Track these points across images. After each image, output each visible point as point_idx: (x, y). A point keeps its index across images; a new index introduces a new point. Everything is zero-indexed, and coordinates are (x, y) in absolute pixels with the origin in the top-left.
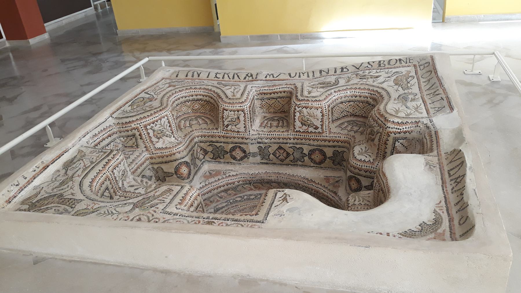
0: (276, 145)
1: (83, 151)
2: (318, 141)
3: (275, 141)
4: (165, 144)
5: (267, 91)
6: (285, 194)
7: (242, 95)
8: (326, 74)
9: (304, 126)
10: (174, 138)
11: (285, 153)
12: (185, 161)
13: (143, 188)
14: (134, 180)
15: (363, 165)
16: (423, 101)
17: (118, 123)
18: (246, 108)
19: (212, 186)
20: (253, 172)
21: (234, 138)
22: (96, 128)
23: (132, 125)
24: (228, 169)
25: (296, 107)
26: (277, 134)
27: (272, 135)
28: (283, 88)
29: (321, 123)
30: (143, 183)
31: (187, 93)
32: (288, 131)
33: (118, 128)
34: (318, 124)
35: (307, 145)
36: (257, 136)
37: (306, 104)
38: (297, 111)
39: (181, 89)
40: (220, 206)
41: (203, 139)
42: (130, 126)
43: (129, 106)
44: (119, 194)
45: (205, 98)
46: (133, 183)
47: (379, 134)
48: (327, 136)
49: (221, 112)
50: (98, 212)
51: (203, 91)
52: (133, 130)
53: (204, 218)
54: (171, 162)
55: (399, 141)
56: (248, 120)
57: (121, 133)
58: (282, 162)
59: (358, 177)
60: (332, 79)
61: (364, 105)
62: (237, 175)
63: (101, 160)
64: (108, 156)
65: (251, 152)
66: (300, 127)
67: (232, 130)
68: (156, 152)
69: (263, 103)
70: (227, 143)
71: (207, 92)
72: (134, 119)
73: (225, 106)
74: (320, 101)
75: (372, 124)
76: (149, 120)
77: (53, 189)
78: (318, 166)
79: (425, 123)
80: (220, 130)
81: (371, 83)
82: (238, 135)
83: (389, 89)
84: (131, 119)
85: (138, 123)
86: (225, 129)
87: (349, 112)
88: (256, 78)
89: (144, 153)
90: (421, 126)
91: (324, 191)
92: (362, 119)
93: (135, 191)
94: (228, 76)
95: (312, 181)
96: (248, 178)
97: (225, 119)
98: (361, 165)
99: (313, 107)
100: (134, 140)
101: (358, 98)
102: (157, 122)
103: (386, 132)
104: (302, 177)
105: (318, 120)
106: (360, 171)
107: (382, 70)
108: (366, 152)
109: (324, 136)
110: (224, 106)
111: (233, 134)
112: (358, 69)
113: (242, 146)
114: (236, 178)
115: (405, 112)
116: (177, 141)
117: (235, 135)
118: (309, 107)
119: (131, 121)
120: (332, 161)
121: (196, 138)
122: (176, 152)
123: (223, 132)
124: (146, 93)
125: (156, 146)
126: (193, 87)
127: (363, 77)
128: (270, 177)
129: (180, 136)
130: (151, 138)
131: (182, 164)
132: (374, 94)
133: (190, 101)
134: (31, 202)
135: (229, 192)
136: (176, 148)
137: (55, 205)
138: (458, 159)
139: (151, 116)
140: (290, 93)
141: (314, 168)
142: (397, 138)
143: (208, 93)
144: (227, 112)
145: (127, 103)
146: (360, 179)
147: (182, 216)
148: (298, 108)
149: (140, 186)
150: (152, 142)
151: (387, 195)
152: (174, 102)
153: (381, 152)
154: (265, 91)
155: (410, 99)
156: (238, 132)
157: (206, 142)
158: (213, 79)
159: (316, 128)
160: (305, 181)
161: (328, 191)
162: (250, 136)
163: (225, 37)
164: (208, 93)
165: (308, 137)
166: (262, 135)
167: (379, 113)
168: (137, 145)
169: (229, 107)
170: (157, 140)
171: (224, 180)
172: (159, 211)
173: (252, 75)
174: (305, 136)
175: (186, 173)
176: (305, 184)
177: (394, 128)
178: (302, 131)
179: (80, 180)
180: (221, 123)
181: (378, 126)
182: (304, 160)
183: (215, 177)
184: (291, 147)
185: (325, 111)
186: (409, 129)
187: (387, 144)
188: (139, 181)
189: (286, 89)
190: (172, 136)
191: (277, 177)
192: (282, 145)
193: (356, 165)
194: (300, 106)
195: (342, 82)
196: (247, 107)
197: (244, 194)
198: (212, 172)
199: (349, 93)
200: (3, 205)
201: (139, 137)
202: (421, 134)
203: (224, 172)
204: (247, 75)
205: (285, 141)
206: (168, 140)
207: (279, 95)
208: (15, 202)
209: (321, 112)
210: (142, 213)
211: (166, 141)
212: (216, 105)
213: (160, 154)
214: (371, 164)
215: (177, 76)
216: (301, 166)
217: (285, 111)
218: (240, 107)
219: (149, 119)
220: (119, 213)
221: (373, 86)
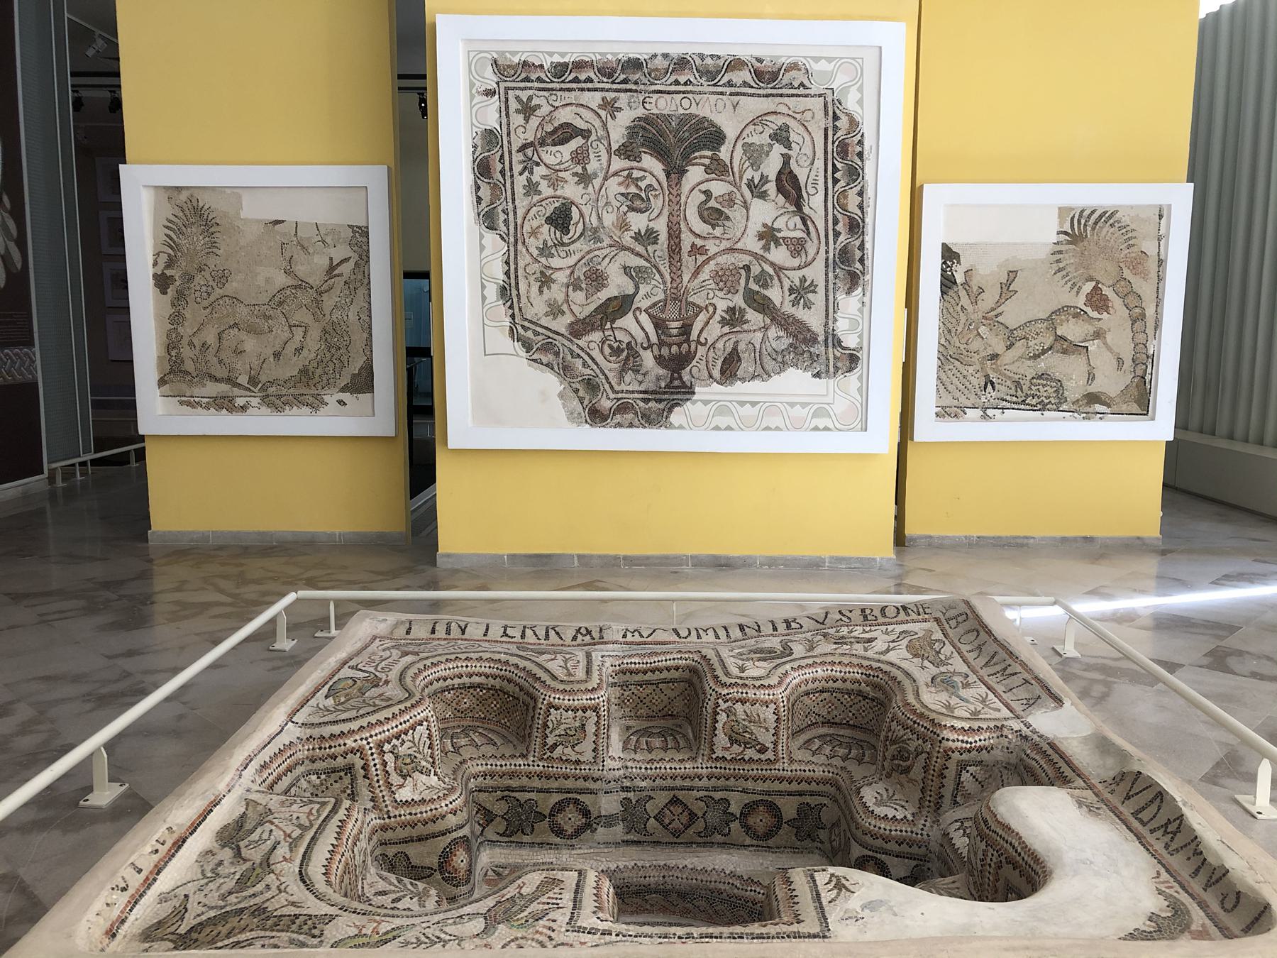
1: (259, 801)
2: (764, 782)
3: (664, 783)
5: (637, 666)
7: (587, 672)
8: (755, 633)
9: (735, 745)
11: (686, 813)
13: (411, 898)
15: (893, 828)
16: (989, 689)
17: (311, 737)
18: (602, 704)
21: (566, 777)
22: (265, 746)
23: (346, 742)
24: (541, 861)
26: (668, 767)
27: (658, 770)
28: (674, 659)
29: (773, 739)
30: (405, 885)
31: (449, 669)
32: (694, 759)
33: (308, 750)
34: (766, 739)
35: (738, 791)
37: (742, 693)
38: (721, 710)
39: (435, 660)
41: (489, 782)
42: (342, 742)
43: (326, 697)
45: (491, 681)
46: (382, 885)
48: (786, 769)
49: (542, 712)
50: (401, 939)
51: (488, 665)
53: (679, 937)
54: (433, 837)
55: (968, 768)
56: (602, 732)
57: (314, 762)
59: (883, 857)
60: (774, 643)
61: (852, 700)
63: (324, 821)
64: (336, 813)
65: (603, 813)
66: (727, 749)
67: (564, 758)
68: (397, 813)
69: (626, 693)
70: (548, 791)
71: (497, 668)
72: (354, 725)
73: (554, 698)
74: (770, 686)
75: (899, 736)
76: (388, 730)
77: (223, 897)
78: (761, 843)
79: (1015, 729)
80: (532, 759)
81: (862, 653)
82: (576, 769)
83: (904, 665)
84: (345, 727)
85: (364, 736)
86: (545, 757)
87: (819, 715)
88: (601, 637)
90: (1010, 736)
92: (848, 731)
93: (395, 905)
94: (535, 633)
95: (752, 880)
97: (550, 729)
98: (888, 828)
99: (757, 701)
100: (347, 780)
101: (839, 684)
102: (406, 735)
104: (727, 872)
105: (768, 731)
106: (886, 842)
107: (873, 628)
108: (890, 798)
109: (779, 770)
110: (552, 699)
111: (564, 770)
112: (823, 624)
113: (581, 797)
115: (965, 708)
116: (443, 785)
117: (568, 770)
118: (748, 700)
119: (346, 732)
120: (795, 830)
121: (472, 780)
122: (446, 812)
123: (541, 764)
124: (351, 668)
125: (397, 796)
126: (463, 656)
127: (840, 641)
128: (645, 877)
130: (389, 775)
131: (457, 843)
132: (874, 676)
133: (453, 689)
134: (173, 933)
136: (448, 803)
137: (254, 934)
138: (1144, 790)
139: (395, 720)
141: (751, 849)
142: (966, 761)
143: (501, 670)
144: (559, 712)
145: (317, 690)
147: (624, 936)
148: (725, 702)
149: (402, 894)
150: (389, 785)
151: (1037, 868)
152: (423, 690)
153: (930, 796)
154: (633, 665)
155: (961, 684)
156: (578, 762)
157: (495, 789)
158: (500, 639)
159: (763, 750)
160: (735, 883)
162: (605, 772)
163: (449, 556)
164: (501, 670)
165: (741, 771)
166: (634, 770)
167: (914, 712)
168: (353, 793)
169: (564, 700)
172: (561, 927)
173: (589, 632)
174: (737, 771)
177: (958, 740)
178: (728, 758)
179: (297, 870)
180: (538, 739)
181: (918, 739)
182: (730, 831)
184: (700, 799)
185: (782, 710)
186: (987, 743)
187: (945, 777)
188: (396, 882)
189: (680, 661)
190: (432, 773)
191: (664, 877)
192: (680, 795)
193: (877, 829)
194: (728, 697)
195: (798, 650)
196: (604, 701)
199: (820, 672)
200: (101, 943)
201: (362, 772)
202: (1012, 752)
204: (578, 631)
205: (687, 783)
207: (665, 674)
208: (125, 937)
209: (774, 713)
210: (520, 935)
212: (522, 697)
213: (408, 817)
214: (909, 824)
215: (408, 632)
216: (723, 845)
217: (675, 713)
218: (589, 701)
219: (390, 727)
220: (460, 940)
221: (869, 659)
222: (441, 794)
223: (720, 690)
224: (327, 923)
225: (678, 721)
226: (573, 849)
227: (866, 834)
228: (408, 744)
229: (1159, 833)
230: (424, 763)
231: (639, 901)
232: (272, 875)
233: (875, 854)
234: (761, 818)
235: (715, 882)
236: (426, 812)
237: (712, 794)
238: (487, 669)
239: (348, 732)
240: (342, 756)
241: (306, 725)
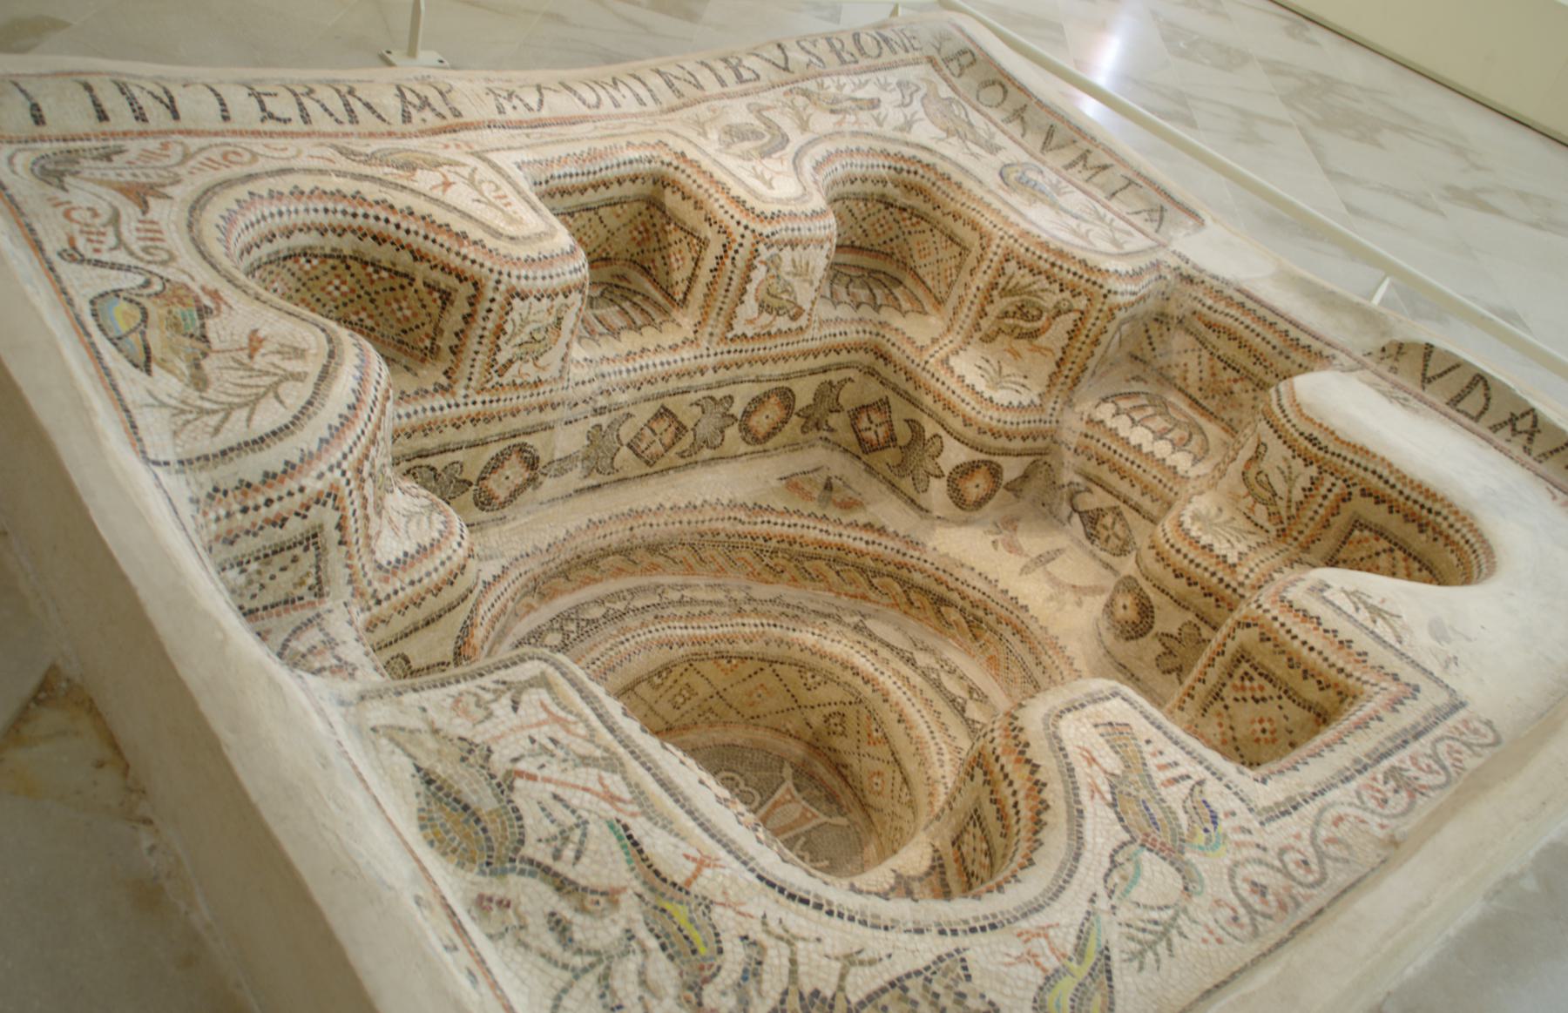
0: (652, 403)
17: (216, 490)
21: (514, 413)
25: (761, 247)
33: (218, 519)
36: (595, 385)
45: (332, 241)
47: (1074, 316)
49: (495, 306)
52: (314, 510)
57: (232, 543)
58: (652, 466)
68: (390, 590)
71: (344, 212)
73: (519, 277)
80: (463, 392)
85: (333, 461)
86: (489, 386)
100: (308, 559)
101: (858, 187)
103: (1105, 308)
104: (725, 502)
105: (811, 283)
119: (296, 460)
123: (479, 399)
140: (655, 183)
144: (527, 302)
146: (1004, 466)
151: (1437, 507)
161: (840, 529)
173: (425, 103)
176: (740, 528)
179: (752, 877)
194: (774, 239)
201: (336, 535)
213: (409, 590)
217: (612, 255)
223: (759, 227)
224: (968, 977)
225: (617, 268)
229: (1507, 431)
232: (717, 911)
236: (436, 570)
237: (714, 393)
238: (321, 214)
239: (302, 460)
240: (297, 514)
241: (190, 462)
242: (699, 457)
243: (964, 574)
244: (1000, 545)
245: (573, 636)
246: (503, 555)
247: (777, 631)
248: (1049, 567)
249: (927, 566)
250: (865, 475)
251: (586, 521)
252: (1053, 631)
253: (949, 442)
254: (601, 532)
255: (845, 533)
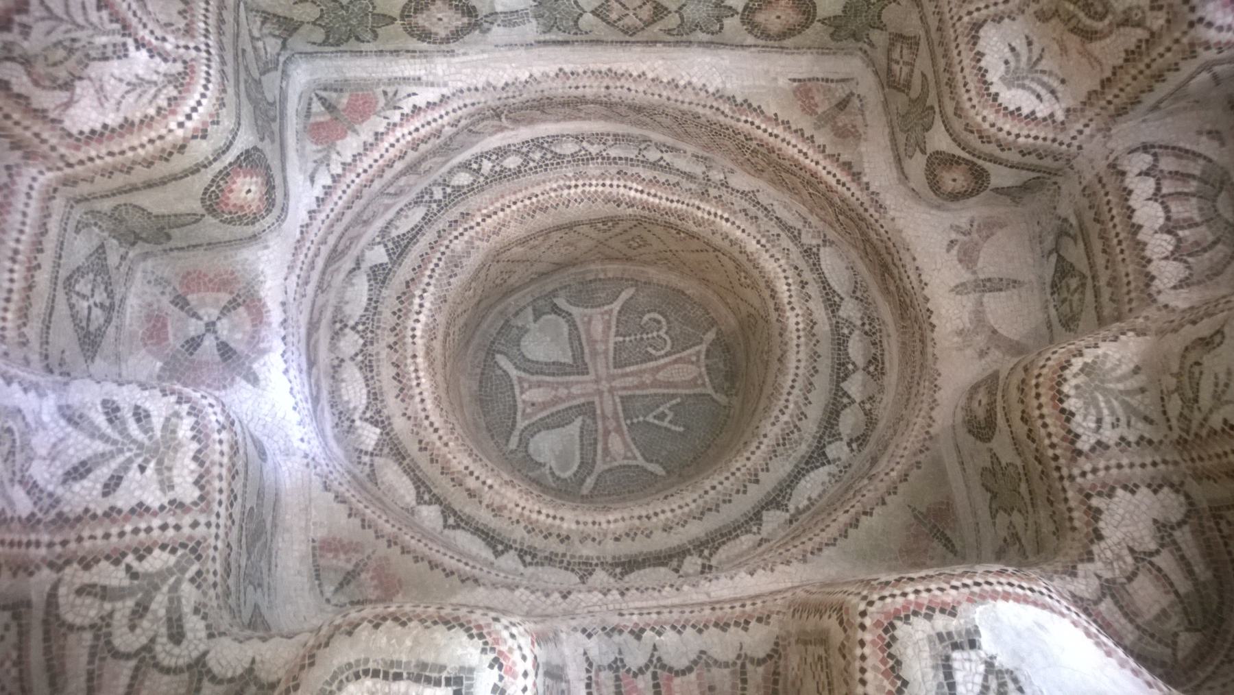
4: (113, 101)
6: (990, 665)
10: (144, 54)
12: (238, 157)
13: (142, 469)
14: (69, 419)
19: (358, 175)
20: (506, 77)
30: (123, 431)
40: (404, 226)
44: (43, 551)
46: (80, 446)
59: (987, 165)
62: (444, 99)
65: (499, 8)
68: (81, 155)
89: (19, 174)
91: (800, 151)
95: (750, 105)
96: (490, 103)
104: (711, 90)
114: (443, 112)
116: (163, 67)
120: (831, 30)
122: (185, 139)
125: (67, 124)
128: (577, 88)
129: (163, 18)
135: (425, 166)
136: (181, 118)
141: (753, 49)
149: (121, 459)
160: (722, 108)
161: (819, 157)
170: (63, 96)
171: (399, 134)
175: (258, 196)
176: (721, 118)
182: (721, 28)
183: (357, 127)
188: (100, 420)
191: (607, 88)
197: (477, 149)
198: (334, 95)
203: (385, 93)
206: (117, 73)
211: (110, 85)
213: (109, 159)
222: (163, 103)
226: (453, 56)
227: (972, 132)
228: (38, 30)
230: (101, 40)
231: (567, 110)
233: (975, 160)
234: (778, 14)
235: (690, 103)
242: (692, 38)
243: (907, 259)
244: (954, 252)
245: (532, 164)
246: (446, 85)
247: (726, 226)
248: (988, 298)
249: (882, 231)
250: (880, 108)
251: (555, 68)
252: (940, 366)
253: (938, 124)
254: (571, 82)
255: (823, 163)
